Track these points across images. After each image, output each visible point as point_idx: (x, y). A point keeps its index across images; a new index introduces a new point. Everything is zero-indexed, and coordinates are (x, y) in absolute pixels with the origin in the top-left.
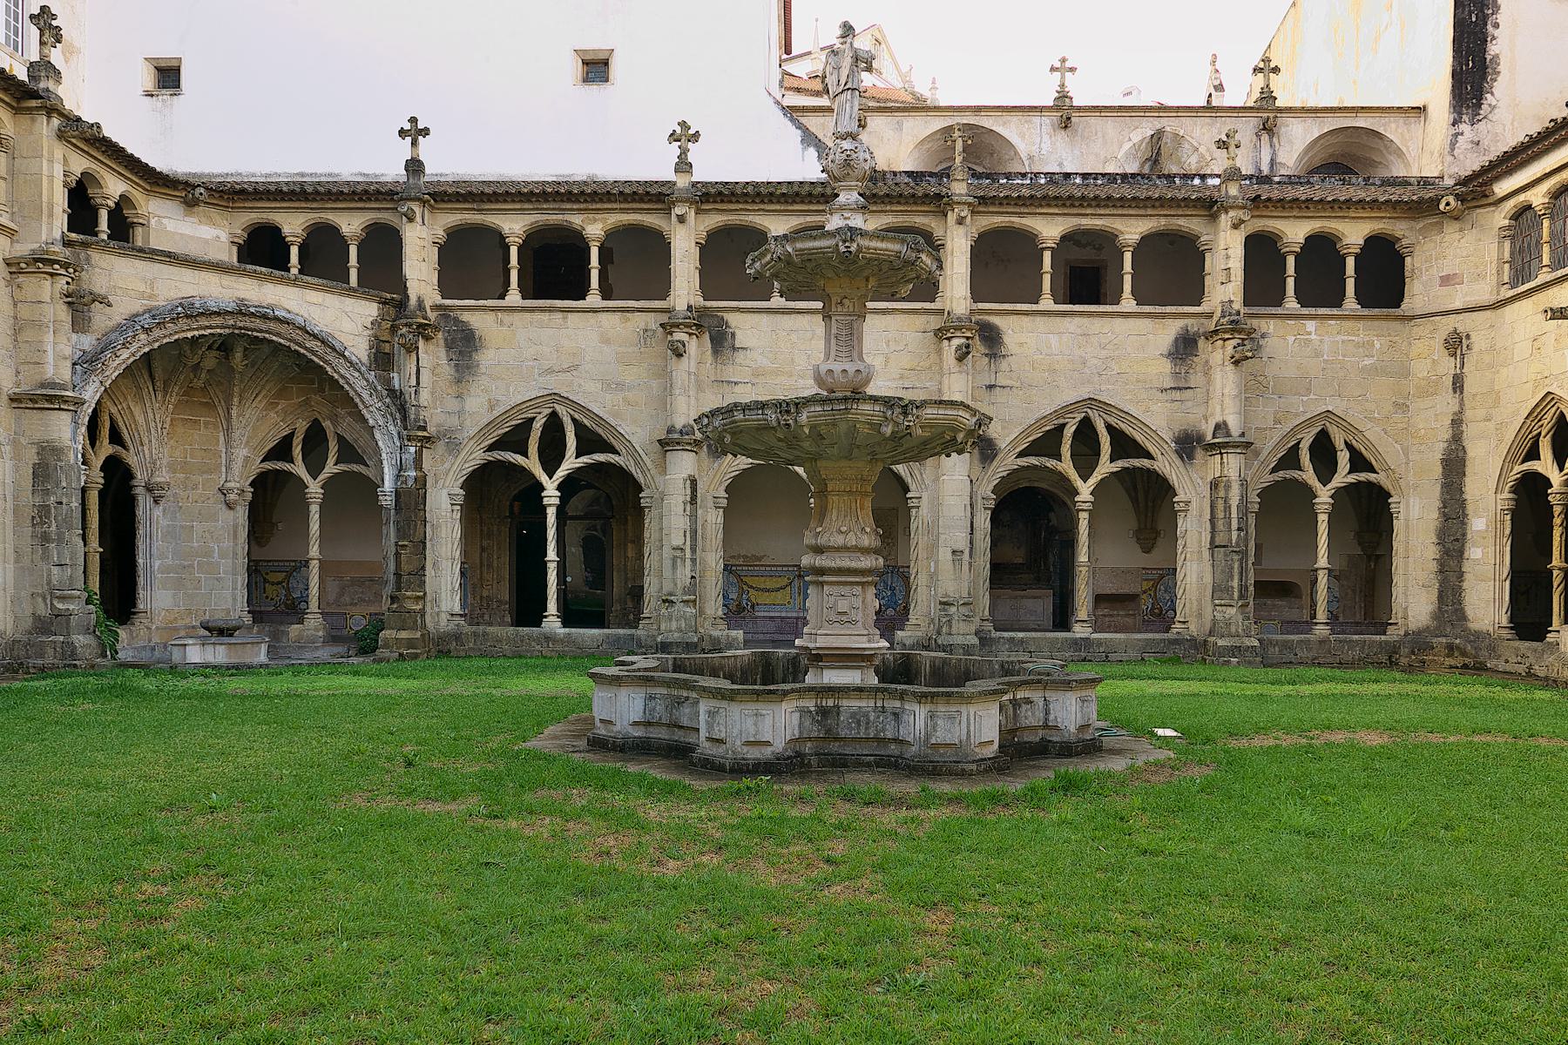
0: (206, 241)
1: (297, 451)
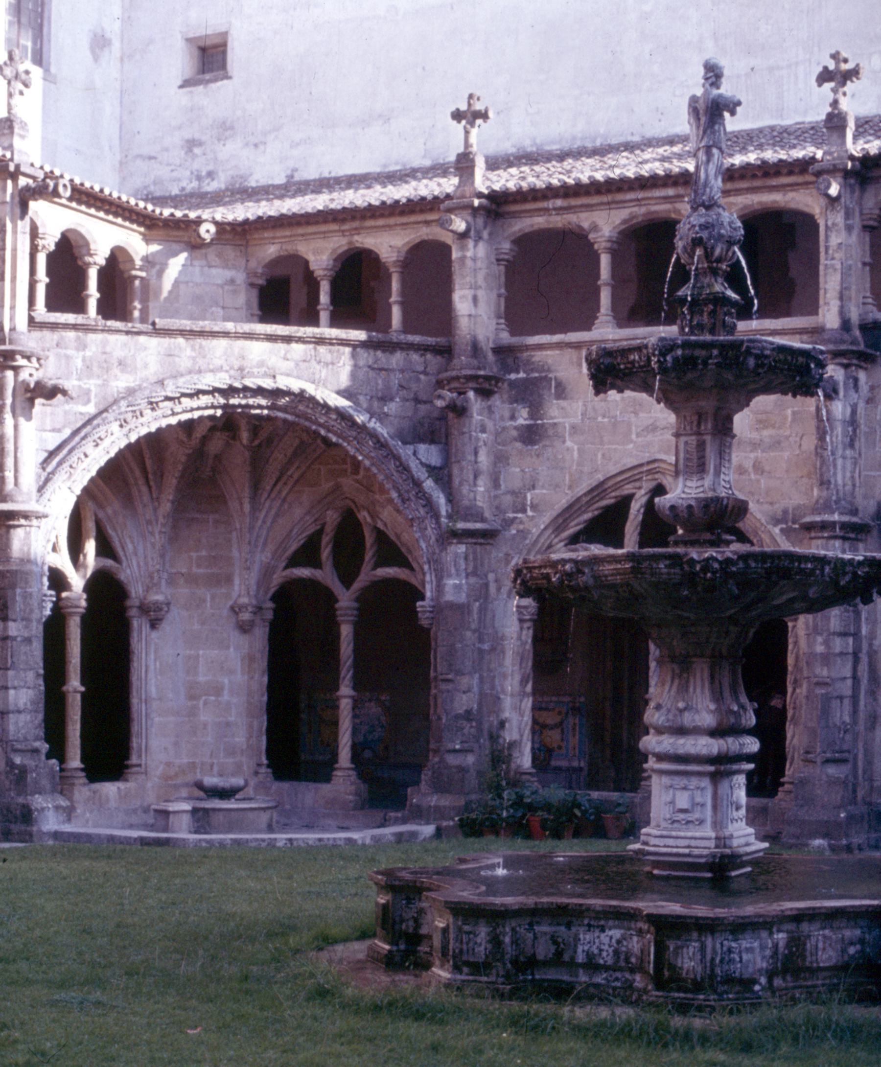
1: (326, 553)
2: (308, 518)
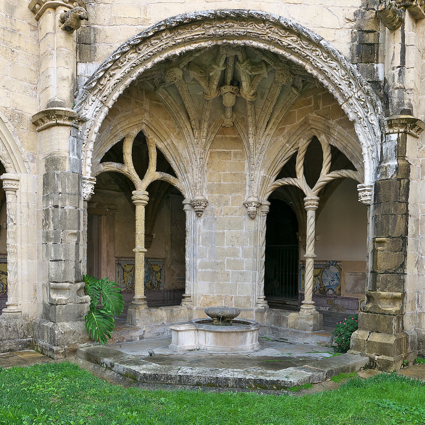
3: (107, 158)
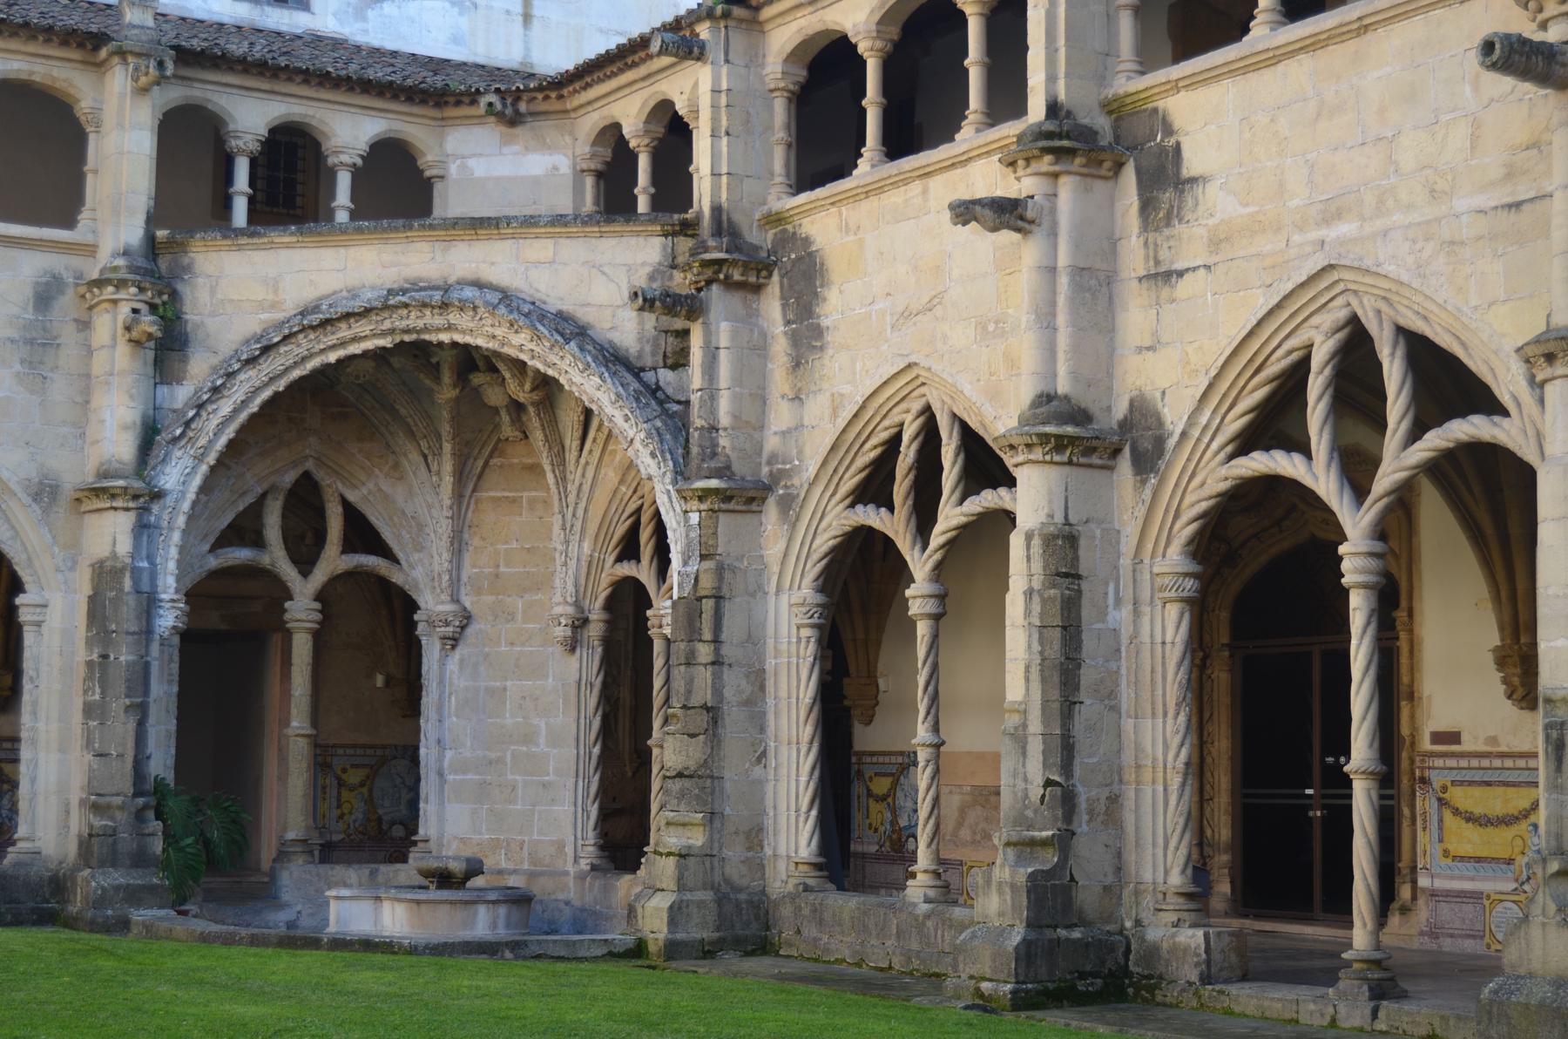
0: (536, 181)
2: (623, 489)
3: (225, 540)
